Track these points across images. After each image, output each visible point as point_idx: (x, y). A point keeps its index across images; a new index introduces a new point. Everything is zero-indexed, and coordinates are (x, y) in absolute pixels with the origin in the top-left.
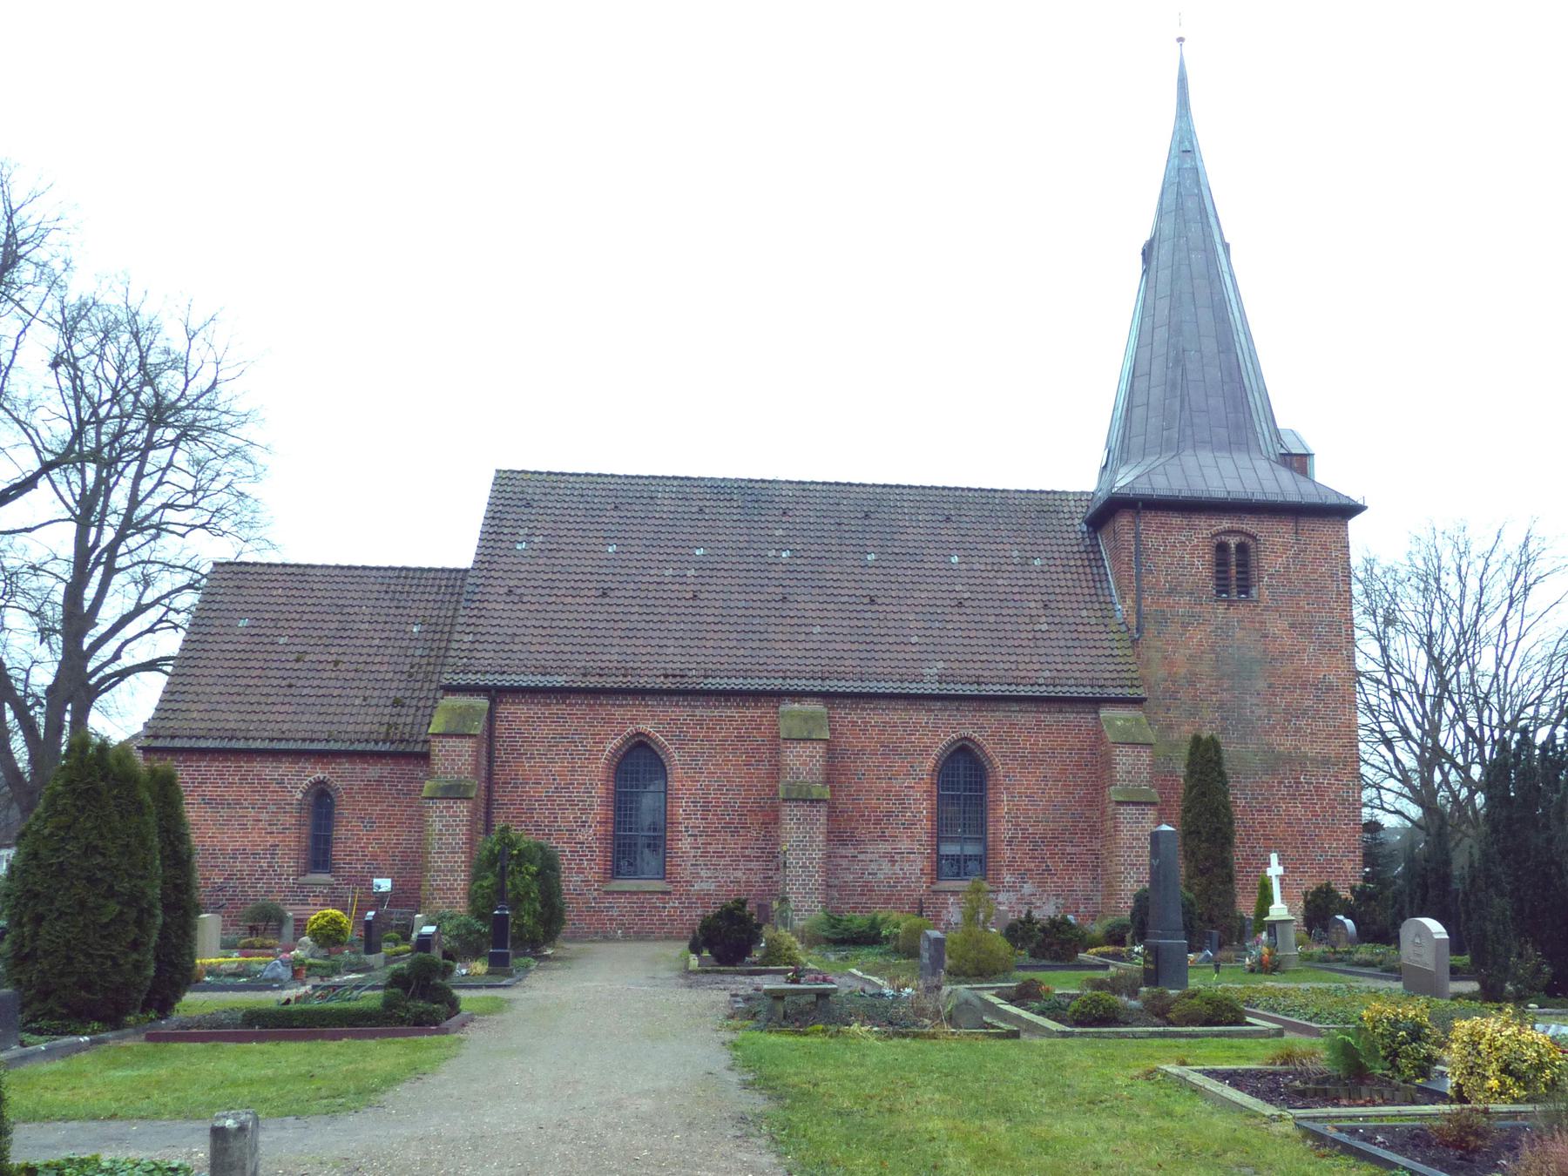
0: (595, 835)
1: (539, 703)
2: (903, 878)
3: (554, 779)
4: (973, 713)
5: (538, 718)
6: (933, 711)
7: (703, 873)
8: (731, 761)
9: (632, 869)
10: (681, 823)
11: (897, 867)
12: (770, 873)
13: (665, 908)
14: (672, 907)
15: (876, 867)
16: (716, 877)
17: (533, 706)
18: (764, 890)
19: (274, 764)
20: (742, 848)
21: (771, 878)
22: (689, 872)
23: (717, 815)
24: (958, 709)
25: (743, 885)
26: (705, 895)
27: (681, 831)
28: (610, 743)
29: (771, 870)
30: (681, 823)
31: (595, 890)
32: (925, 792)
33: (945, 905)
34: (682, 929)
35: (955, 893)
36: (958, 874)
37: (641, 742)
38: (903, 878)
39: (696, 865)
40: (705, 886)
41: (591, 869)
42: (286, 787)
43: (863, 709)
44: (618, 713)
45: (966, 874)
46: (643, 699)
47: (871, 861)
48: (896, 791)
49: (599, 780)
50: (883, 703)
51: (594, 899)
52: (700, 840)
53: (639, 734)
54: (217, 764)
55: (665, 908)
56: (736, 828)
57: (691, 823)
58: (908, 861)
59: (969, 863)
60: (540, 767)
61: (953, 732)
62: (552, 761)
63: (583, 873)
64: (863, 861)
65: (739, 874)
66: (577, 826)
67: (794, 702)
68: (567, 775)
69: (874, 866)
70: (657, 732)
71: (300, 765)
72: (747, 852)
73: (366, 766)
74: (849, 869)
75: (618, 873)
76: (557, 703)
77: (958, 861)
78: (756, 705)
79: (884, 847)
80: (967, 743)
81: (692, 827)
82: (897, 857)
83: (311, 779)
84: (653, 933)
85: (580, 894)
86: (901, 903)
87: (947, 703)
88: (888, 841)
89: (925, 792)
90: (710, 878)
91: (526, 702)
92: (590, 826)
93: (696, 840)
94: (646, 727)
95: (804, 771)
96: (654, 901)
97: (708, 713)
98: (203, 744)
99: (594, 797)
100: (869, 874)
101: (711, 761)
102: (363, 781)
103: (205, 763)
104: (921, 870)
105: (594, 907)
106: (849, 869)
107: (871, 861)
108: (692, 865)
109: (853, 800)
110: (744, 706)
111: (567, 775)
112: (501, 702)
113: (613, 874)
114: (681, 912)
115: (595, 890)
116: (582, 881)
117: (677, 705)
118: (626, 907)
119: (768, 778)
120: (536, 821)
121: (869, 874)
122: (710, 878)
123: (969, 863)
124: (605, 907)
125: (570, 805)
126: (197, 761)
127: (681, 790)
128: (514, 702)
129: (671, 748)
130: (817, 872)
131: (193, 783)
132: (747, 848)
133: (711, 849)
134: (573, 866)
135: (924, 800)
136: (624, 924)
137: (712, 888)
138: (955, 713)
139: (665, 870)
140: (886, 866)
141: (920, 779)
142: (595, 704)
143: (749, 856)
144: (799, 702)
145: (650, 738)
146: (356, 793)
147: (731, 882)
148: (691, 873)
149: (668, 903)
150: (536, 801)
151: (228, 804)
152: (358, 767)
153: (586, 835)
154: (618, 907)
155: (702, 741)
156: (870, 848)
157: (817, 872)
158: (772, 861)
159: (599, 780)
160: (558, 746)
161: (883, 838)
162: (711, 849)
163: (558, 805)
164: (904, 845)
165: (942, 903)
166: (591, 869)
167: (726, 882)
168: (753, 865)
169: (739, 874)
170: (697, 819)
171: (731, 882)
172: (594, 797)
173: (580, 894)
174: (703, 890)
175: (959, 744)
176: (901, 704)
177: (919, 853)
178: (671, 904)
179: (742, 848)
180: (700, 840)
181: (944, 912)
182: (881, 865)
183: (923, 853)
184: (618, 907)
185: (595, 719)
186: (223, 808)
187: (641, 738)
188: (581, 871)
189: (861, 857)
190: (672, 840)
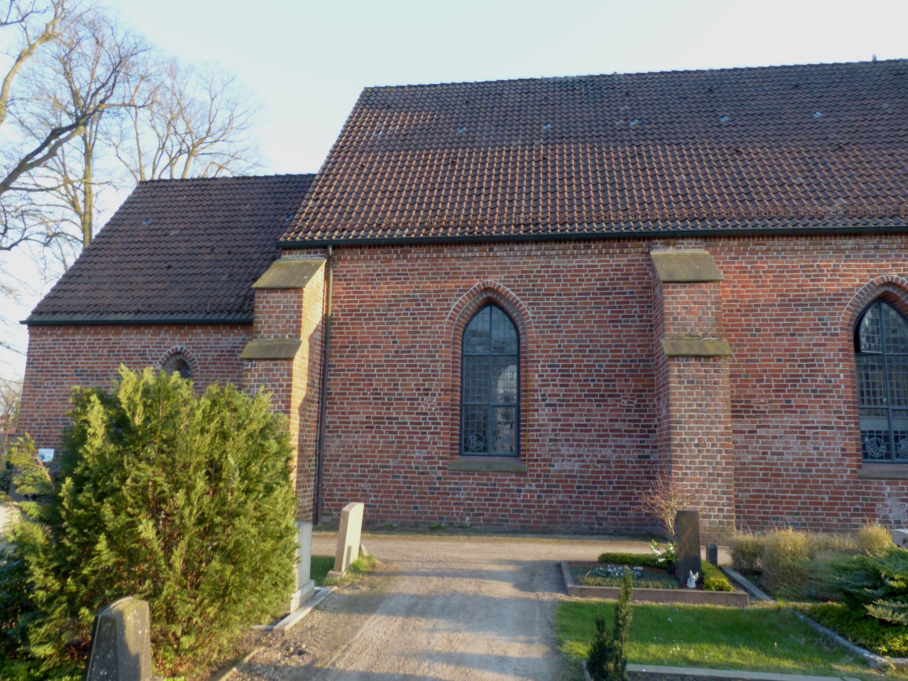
0: (439, 404)
1: (378, 258)
2: (818, 460)
3: (394, 342)
4: (897, 252)
5: (378, 275)
6: (843, 251)
7: (564, 451)
8: (594, 317)
9: (481, 444)
10: (536, 391)
11: (809, 446)
12: (647, 452)
13: (520, 491)
14: (528, 491)
15: (781, 445)
16: (579, 456)
17: (372, 263)
18: (640, 473)
19: (138, 337)
20: (611, 420)
21: (648, 457)
22: (547, 448)
23: (580, 381)
24: (876, 248)
25: (613, 465)
26: (566, 476)
27: (537, 400)
28: (455, 300)
29: (648, 447)
30: (536, 391)
31: (439, 468)
32: (840, 350)
33: (879, 496)
34: (540, 517)
35: (892, 481)
36: (888, 456)
37: (489, 298)
38: (818, 460)
39: (556, 440)
40: (566, 466)
41: (435, 443)
42: (147, 359)
43: (753, 252)
44: (464, 266)
45: (898, 455)
46: (491, 250)
47: (775, 437)
48: (801, 350)
49: (443, 342)
50: (778, 243)
51: (439, 478)
52: (560, 412)
53: (486, 289)
54: (89, 337)
55: (520, 491)
56: (601, 396)
57: (549, 390)
58: (823, 438)
59: (901, 442)
60: (379, 328)
61: (872, 276)
62: (391, 321)
63: (426, 448)
64: (763, 437)
65: (608, 452)
66: (419, 394)
67: (668, 245)
68: (408, 337)
69: (778, 445)
70: (508, 286)
71: (161, 336)
72: (617, 425)
73: (220, 336)
74: (747, 447)
75: (466, 449)
76: (398, 258)
77: (887, 439)
78: (622, 252)
79: (789, 420)
80: (891, 290)
81: (550, 395)
82: (809, 433)
83: (170, 350)
84: (507, 521)
85: (423, 473)
86: (820, 493)
87: (861, 241)
88: (796, 412)
89: (840, 350)
90: (573, 456)
91: (365, 258)
92: (433, 395)
93: (555, 410)
94: (492, 281)
95: (692, 319)
96: (507, 482)
97: (565, 262)
98: (78, 318)
99: (437, 361)
100: (773, 454)
101: (571, 317)
102: (217, 351)
103: (79, 337)
104: (843, 449)
105: (439, 488)
106: (747, 447)
107: (775, 437)
108: (551, 440)
109: (747, 361)
110: (608, 253)
111: (408, 337)
112: (339, 259)
113: (460, 449)
114: (540, 497)
115: (439, 468)
116: (425, 458)
117: (529, 256)
118: (474, 489)
119: (639, 336)
120: (376, 389)
121: (773, 454)
122: (573, 456)
123: (901, 442)
124: (451, 489)
125: (412, 371)
126: (73, 334)
127: (537, 351)
128: (352, 259)
129: (524, 305)
130: (720, 452)
131: (68, 355)
132: (617, 421)
133: (573, 421)
134: (414, 440)
135: (840, 360)
136: (472, 510)
137: (576, 468)
138: (872, 252)
139: (518, 446)
140: (794, 442)
141: (832, 335)
142: (438, 257)
143: (620, 430)
144: (674, 245)
145: (499, 294)
146: (210, 363)
147: (599, 462)
148: (550, 450)
149: (524, 486)
150: (375, 366)
151: (97, 375)
152: (213, 337)
153: (429, 404)
154: (465, 489)
155: (560, 295)
156: (772, 422)
157: (720, 452)
158: (648, 436)
159: (443, 342)
160: (398, 305)
161: (787, 407)
162: (573, 421)
163: (399, 371)
164: (817, 417)
165: (874, 494)
166: (435, 443)
167: (592, 461)
168: (624, 441)
169: (608, 452)
170: (555, 385)
171: (599, 462)
172: (437, 361)
173: (423, 473)
174: (565, 471)
175: (879, 292)
176: (802, 244)
177: (838, 428)
178: (527, 487)
179: (611, 420)
180: (560, 412)
181: (879, 505)
182: (787, 443)
183: (844, 428)
184: (465, 489)
185: (438, 274)
186: (92, 380)
187: (490, 295)
188: (423, 446)
189: (761, 432)
190: (525, 411)
